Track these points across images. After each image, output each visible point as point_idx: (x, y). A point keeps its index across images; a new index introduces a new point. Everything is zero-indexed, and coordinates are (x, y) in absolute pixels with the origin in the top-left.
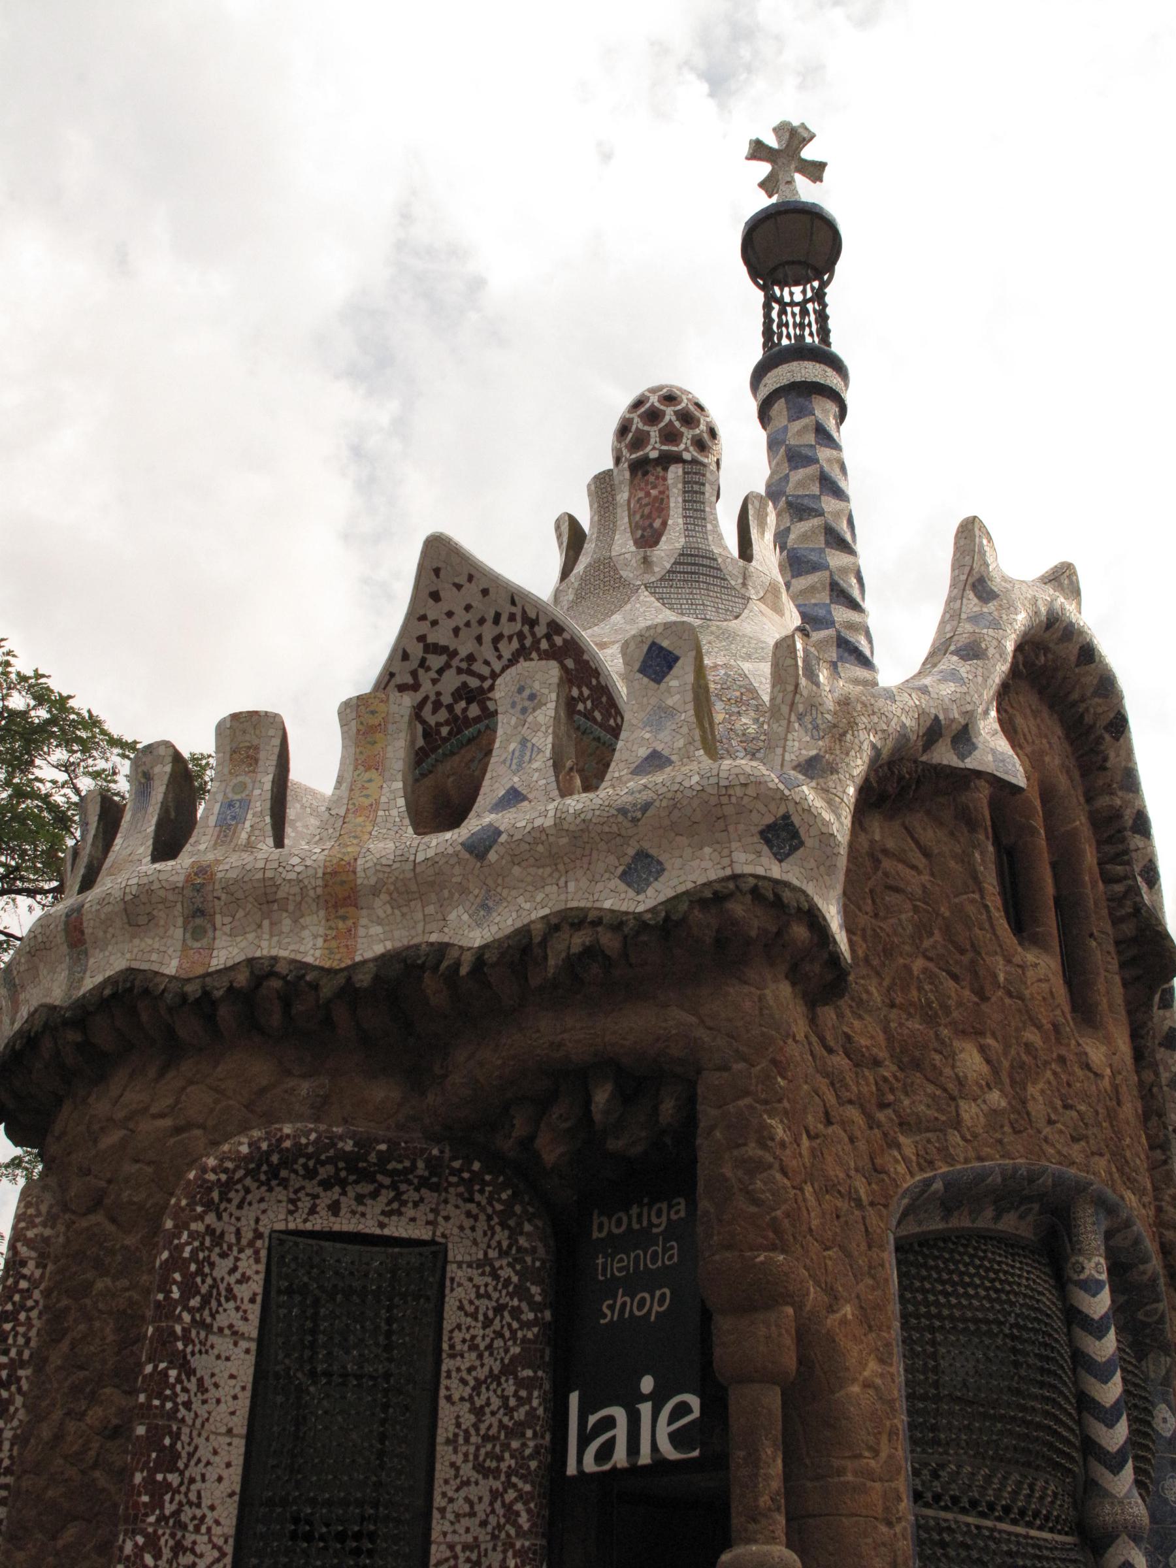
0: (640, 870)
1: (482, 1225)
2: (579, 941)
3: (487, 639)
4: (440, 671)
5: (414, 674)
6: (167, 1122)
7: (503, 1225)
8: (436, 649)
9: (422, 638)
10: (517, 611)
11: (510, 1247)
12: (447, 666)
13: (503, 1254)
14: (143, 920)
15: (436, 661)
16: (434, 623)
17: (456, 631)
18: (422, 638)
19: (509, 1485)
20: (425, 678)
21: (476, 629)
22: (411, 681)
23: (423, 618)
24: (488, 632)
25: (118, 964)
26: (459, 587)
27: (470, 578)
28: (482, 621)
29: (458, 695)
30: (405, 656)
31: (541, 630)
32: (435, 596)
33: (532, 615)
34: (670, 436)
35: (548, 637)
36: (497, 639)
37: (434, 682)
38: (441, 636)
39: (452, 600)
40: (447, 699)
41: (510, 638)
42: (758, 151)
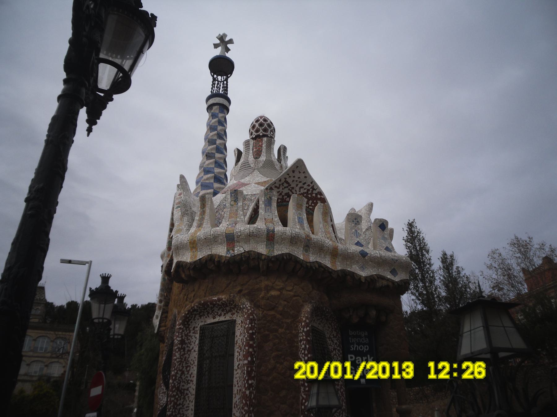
0: (394, 272)
1: (330, 330)
2: (385, 283)
3: (299, 186)
4: (285, 187)
5: (280, 185)
6: (292, 293)
8: (286, 182)
9: (285, 179)
10: (311, 185)
12: (287, 187)
13: (334, 337)
14: (294, 242)
15: (285, 185)
16: (290, 177)
17: (293, 181)
18: (285, 179)
19: (341, 388)
20: (281, 187)
21: (298, 183)
22: (278, 186)
23: (288, 174)
24: (300, 185)
25: (285, 251)
26: (300, 172)
28: (300, 182)
29: (286, 194)
30: (280, 181)
31: (314, 192)
32: (293, 172)
33: (315, 188)
34: (265, 130)
35: (316, 194)
36: (301, 188)
37: (283, 189)
38: (290, 180)
39: (297, 174)
40: (283, 194)
41: (305, 189)
42: (231, 41)
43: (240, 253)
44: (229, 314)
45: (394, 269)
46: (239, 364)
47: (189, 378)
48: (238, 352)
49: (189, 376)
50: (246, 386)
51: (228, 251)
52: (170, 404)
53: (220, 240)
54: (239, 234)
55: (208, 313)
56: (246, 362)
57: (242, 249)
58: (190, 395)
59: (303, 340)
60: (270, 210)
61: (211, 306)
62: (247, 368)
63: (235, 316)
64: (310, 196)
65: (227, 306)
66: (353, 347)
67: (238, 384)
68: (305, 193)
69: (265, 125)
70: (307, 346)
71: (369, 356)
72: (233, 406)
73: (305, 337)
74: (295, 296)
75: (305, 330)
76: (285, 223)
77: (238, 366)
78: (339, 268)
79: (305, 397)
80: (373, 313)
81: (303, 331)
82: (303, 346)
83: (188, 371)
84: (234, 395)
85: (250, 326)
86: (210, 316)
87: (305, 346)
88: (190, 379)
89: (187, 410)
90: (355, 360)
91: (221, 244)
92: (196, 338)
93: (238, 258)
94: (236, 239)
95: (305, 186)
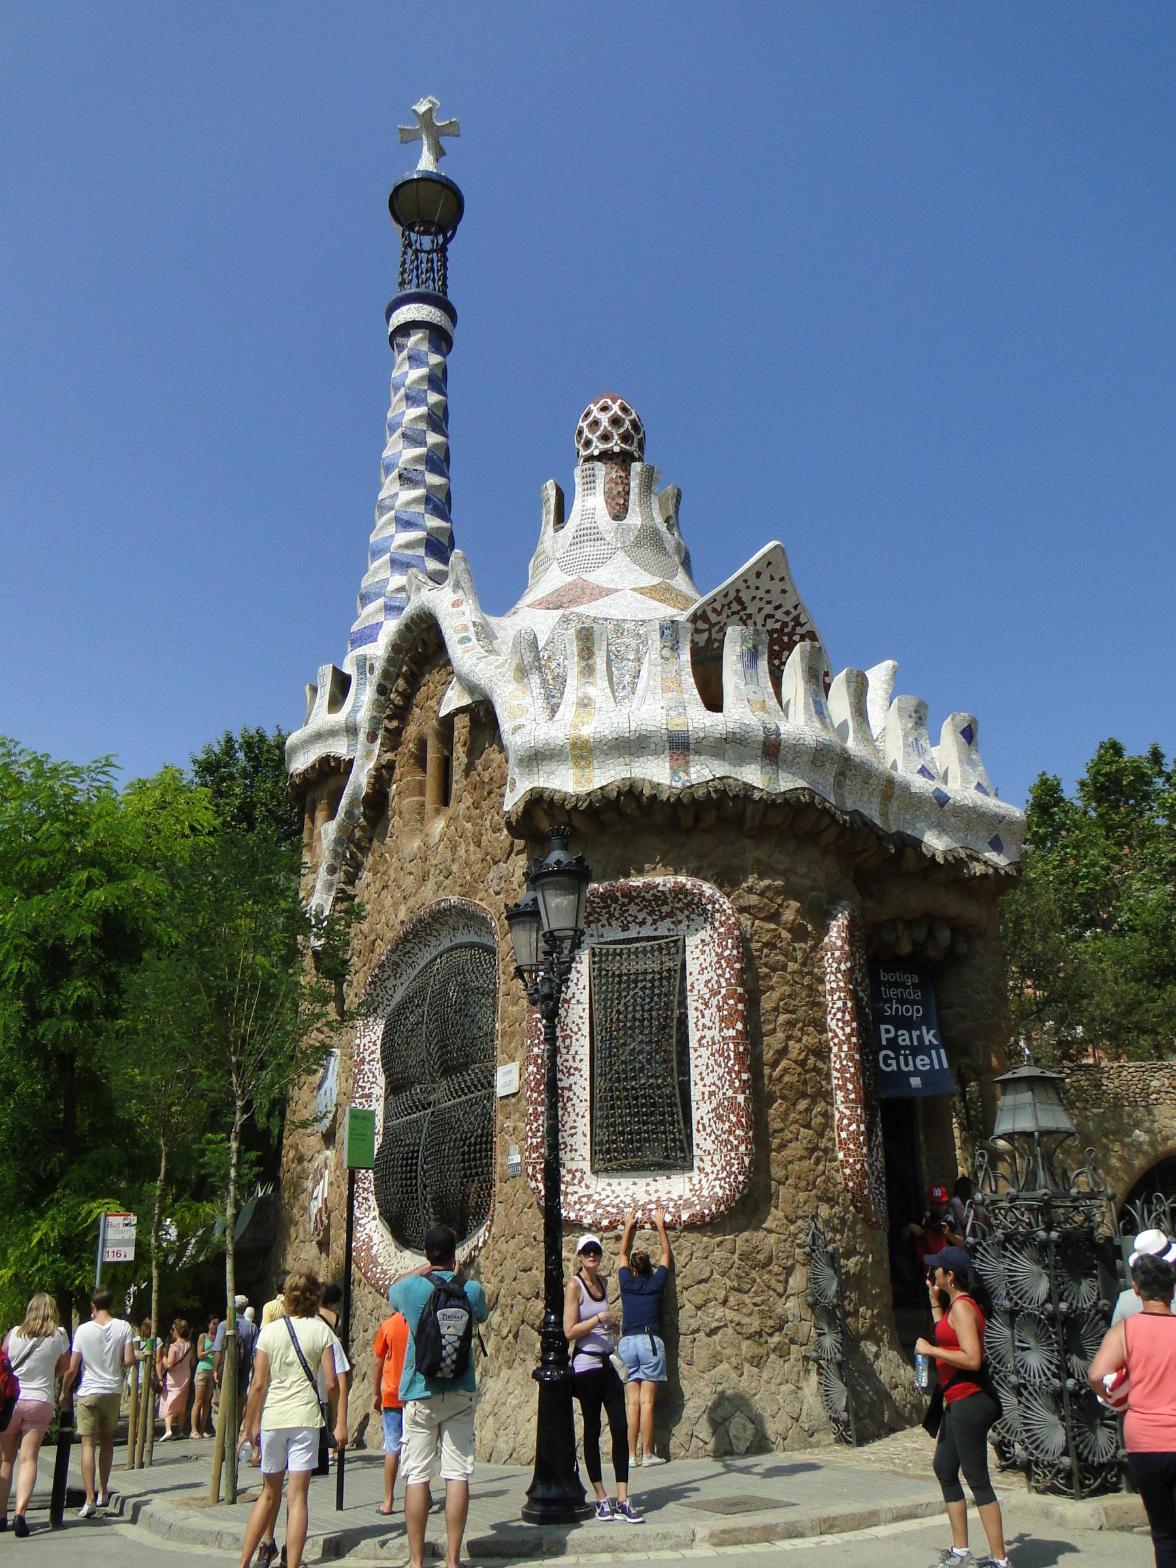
4: (733, 613)
5: (723, 606)
7: (860, 971)
8: (739, 600)
10: (794, 613)
11: (862, 981)
12: (737, 613)
14: (819, 764)
15: (736, 607)
16: (748, 587)
17: (754, 598)
18: (738, 591)
20: (726, 612)
23: (745, 581)
24: (768, 609)
26: (772, 578)
27: (782, 579)
28: (769, 602)
30: (726, 595)
31: (799, 630)
33: (802, 620)
36: (768, 616)
37: (728, 617)
38: (745, 596)
43: (703, 780)
44: (668, 922)
45: (997, 838)
46: (703, 1037)
47: (571, 1063)
48: (696, 1009)
49: (570, 1057)
50: (737, 1085)
51: (674, 772)
52: (536, 1120)
53: (653, 746)
54: (702, 735)
55: (612, 916)
56: (732, 1032)
57: (706, 771)
58: (575, 1101)
59: (839, 989)
60: (755, 680)
61: (622, 900)
62: (737, 1045)
63: (683, 926)
64: (786, 639)
65: (665, 902)
66: (891, 1008)
67: (702, 1079)
68: (776, 630)
69: (627, 425)
70: (849, 1004)
71: (924, 1028)
72: (694, 1127)
73: (842, 984)
74: (813, 888)
75: (843, 967)
76: (713, 702)
77: (699, 1041)
78: (894, 829)
79: (848, 1112)
80: (945, 935)
81: (838, 970)
82: (840, 1004)
83: (568, 1048)
84: (693, 1104)
85: (735, 952)
86: (614, 923)
87: (845, 1004)
88: (574, 1065)
89: (572, 1135)
90: (896, 1036)
91: (655, 753)
92: (578, 972)
93: (700, 793)
94: (692, 746)
95: (779, 614)
